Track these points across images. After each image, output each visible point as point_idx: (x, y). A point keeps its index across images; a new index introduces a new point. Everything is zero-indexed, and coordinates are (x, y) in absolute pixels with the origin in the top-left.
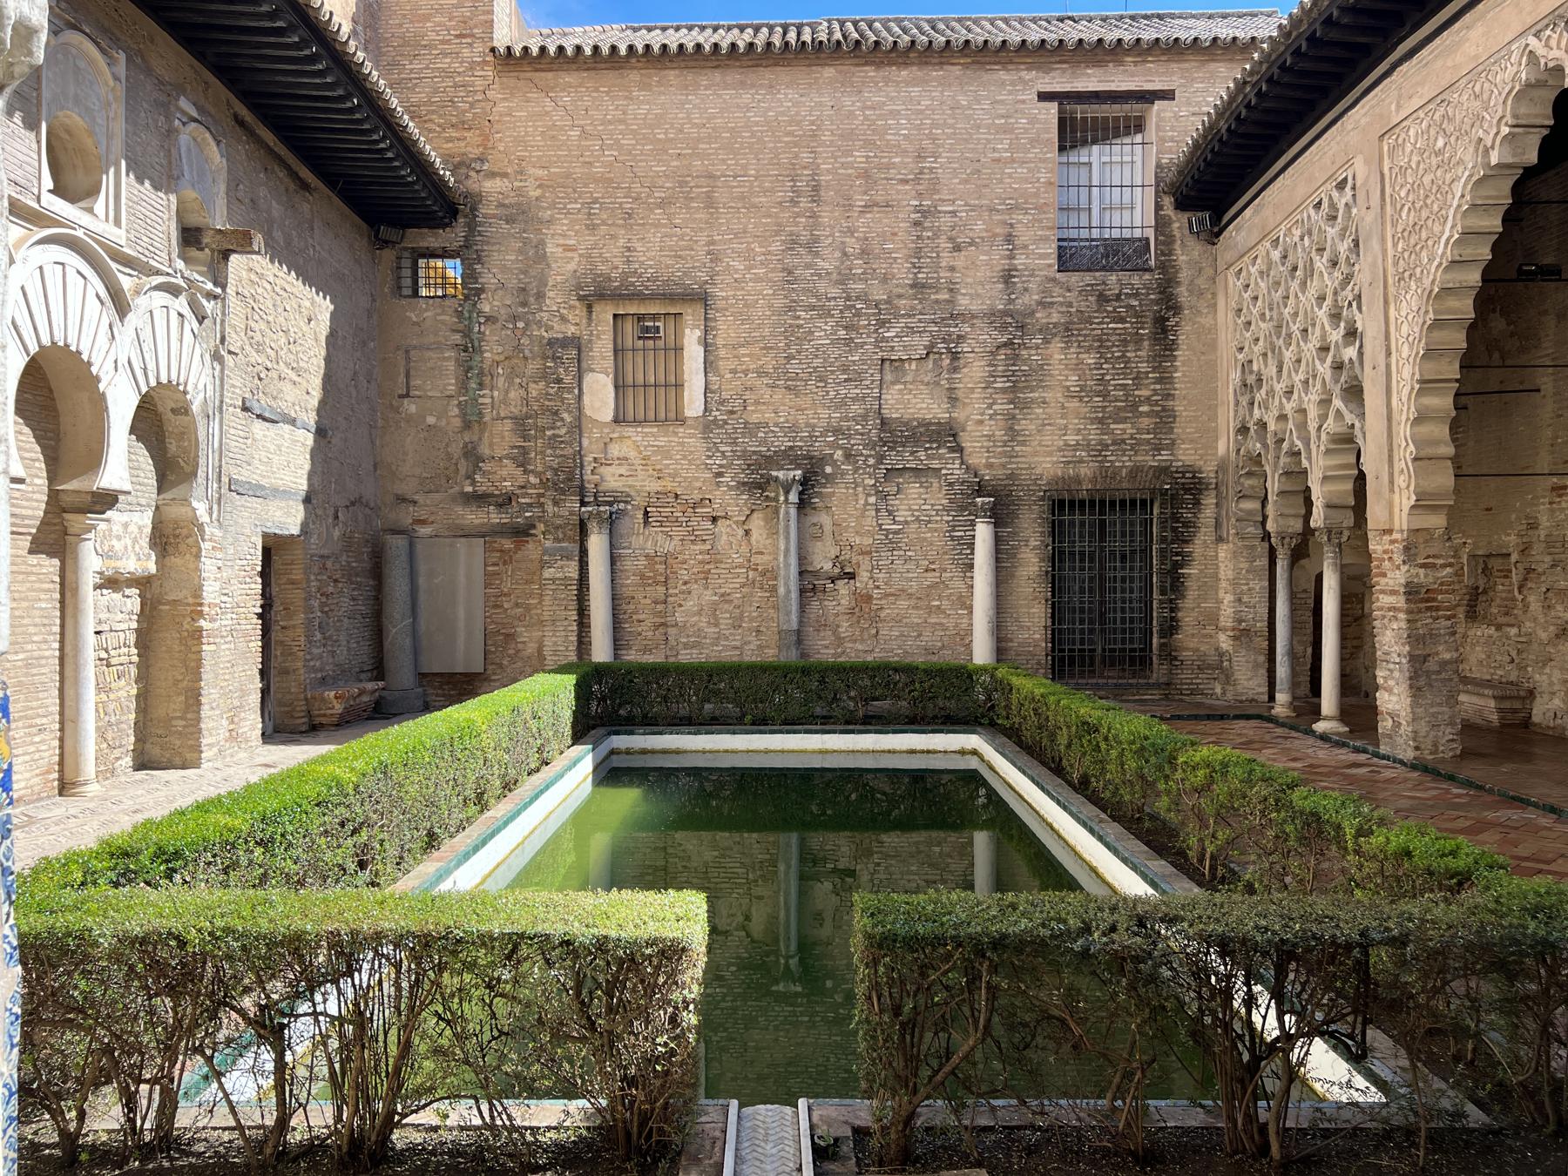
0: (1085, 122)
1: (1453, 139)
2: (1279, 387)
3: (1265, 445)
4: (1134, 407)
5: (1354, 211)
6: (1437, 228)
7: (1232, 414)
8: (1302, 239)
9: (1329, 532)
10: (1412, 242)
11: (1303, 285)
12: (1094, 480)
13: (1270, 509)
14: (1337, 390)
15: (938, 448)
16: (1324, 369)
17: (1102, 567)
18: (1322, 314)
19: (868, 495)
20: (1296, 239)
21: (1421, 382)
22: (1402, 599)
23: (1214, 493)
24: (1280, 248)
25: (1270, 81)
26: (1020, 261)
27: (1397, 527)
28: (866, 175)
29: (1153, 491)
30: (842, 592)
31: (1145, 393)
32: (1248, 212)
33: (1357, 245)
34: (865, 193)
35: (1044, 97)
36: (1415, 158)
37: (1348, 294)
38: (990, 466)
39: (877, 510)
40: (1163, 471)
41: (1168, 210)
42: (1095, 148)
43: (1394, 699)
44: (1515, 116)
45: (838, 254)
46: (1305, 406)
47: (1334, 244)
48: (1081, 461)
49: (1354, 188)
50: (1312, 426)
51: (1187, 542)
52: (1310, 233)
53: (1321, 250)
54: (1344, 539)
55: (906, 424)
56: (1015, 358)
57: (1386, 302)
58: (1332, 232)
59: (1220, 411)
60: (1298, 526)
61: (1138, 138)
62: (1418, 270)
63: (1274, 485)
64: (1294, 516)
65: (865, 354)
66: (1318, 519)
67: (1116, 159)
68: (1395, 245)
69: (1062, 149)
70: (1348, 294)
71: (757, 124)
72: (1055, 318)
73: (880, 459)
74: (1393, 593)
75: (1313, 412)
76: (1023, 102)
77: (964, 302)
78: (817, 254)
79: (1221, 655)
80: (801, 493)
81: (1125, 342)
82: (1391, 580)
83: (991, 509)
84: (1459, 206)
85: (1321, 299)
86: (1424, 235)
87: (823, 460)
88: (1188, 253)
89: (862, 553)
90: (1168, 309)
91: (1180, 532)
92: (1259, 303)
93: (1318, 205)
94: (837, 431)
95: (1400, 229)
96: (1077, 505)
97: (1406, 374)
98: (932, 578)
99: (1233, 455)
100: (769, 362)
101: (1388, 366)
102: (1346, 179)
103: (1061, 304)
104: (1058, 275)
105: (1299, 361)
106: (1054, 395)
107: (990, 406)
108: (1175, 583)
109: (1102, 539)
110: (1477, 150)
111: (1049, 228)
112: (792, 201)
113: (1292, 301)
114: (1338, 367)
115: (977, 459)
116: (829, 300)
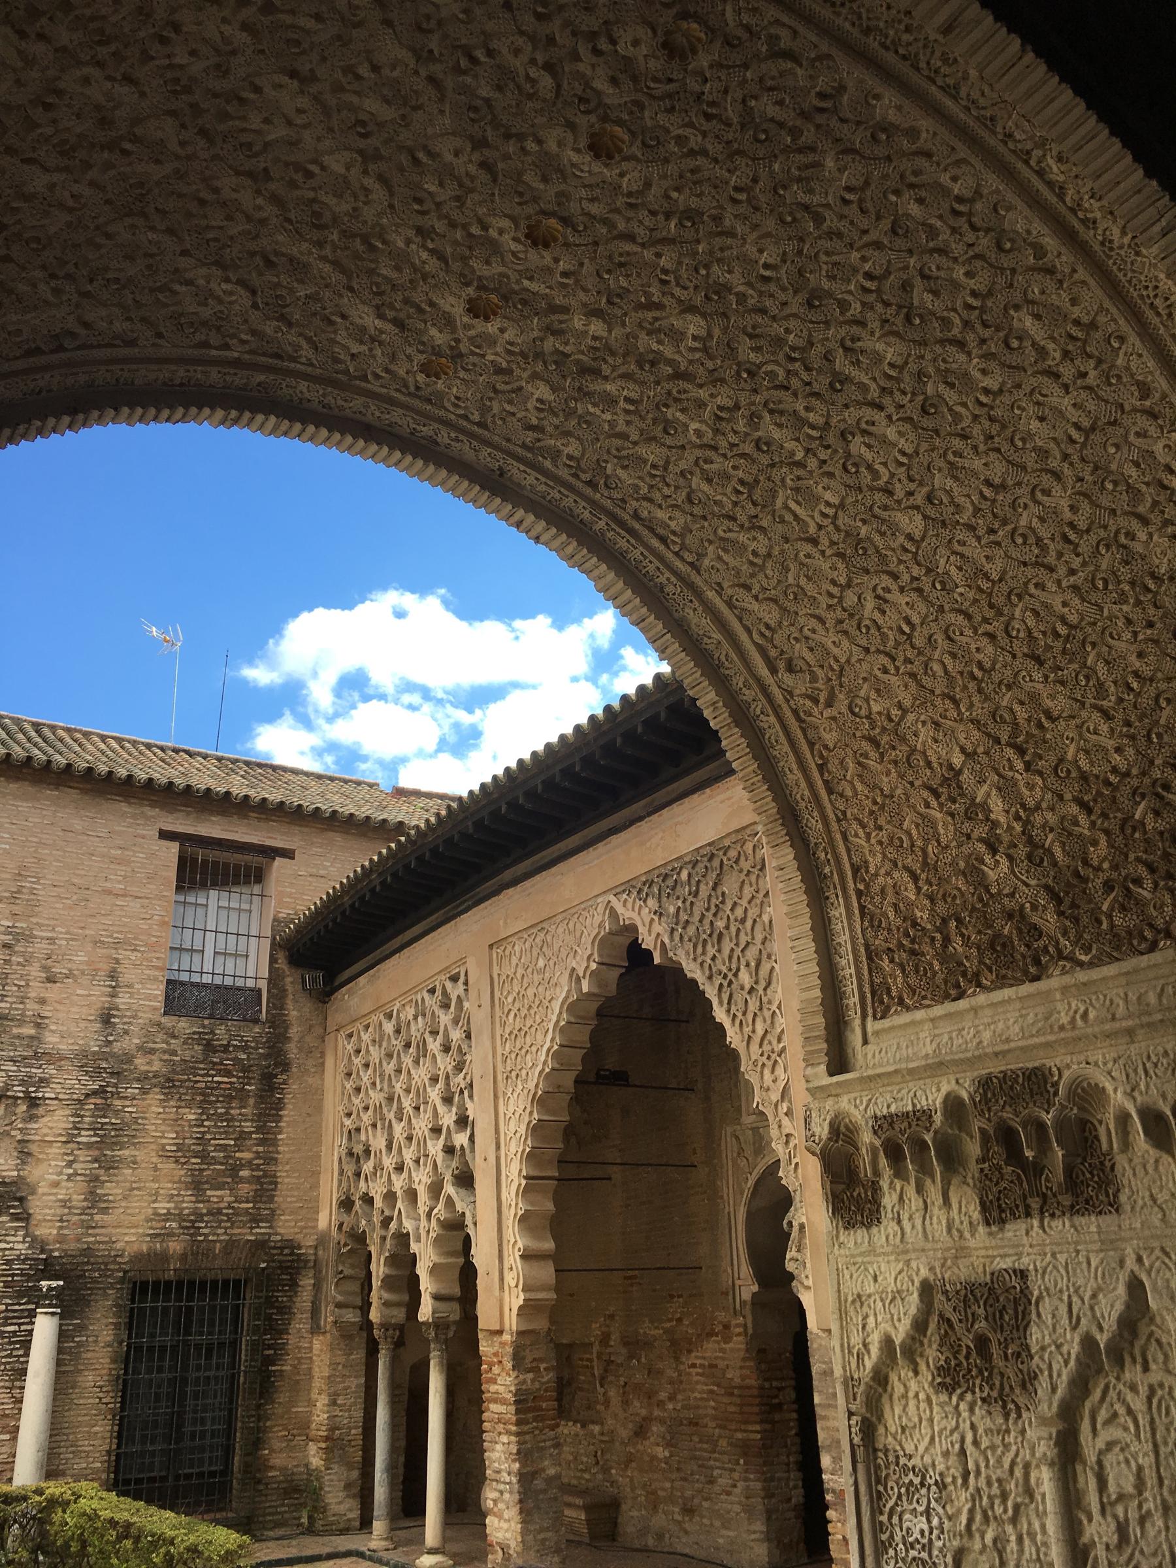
0: (207, 868)
2: (388, 1162)
3: (369, 1221)
4: (234, 1170)
5: (466, 1005)
6: (540, 1036)
8: (416, 1018)
10: (518, 1046)
12: (183, 1257)
13: (376, 1295)
14: (448, 1177)
16: (435, 1148)
17: (185, 1368)
20: (411, 1017)
22: (512, 1409)
23: (311, 1273)
24: (394, 1021)
25: (395, 875)
26: (122, 1000)
27: (507, 1327)
31: (247, 1155)
32: (362, 980)
33: (468, 1036)
35: (165, 835)
36: (520, 971)
37: (459, 1080)
40: (261, 1245)
41: (282, 964)
42: (213, 893)
43: (505, 1525)
44: (600, 955)
49: (466, 983)
50: (422, 1208)
52: (424, 1015)
53: (435, 1033)
54: (451, 1334)
58: (445, 1018)
61: (257, 889)
62: (524, 1072)
63: (379, 1269)
64: (398, 1304)
66: (426, 1310)
69: (179, 888)
70: (459, 1080)
72: (157, 1066)
74: (503, 1402)
75: (423, 1197)
76: (143, 837)
77: (51, 1040)
82: (501, 1385)
83: (57, 1297)
84: (558, 1022)
85: (434, 1080)
88: (297, 1011)
90: (276, 1065)
91: (274, 1322)
95: (507, 1031)
96: (162, 1288)
97: (515, 1172)
101: (498, 1159)
103: (165, 1052)
104: (163, 1020)
108: (265, 1383)
109: (187, 1332)
110: (571, 976)
113: (404, 1075)
114: (449, 1150)
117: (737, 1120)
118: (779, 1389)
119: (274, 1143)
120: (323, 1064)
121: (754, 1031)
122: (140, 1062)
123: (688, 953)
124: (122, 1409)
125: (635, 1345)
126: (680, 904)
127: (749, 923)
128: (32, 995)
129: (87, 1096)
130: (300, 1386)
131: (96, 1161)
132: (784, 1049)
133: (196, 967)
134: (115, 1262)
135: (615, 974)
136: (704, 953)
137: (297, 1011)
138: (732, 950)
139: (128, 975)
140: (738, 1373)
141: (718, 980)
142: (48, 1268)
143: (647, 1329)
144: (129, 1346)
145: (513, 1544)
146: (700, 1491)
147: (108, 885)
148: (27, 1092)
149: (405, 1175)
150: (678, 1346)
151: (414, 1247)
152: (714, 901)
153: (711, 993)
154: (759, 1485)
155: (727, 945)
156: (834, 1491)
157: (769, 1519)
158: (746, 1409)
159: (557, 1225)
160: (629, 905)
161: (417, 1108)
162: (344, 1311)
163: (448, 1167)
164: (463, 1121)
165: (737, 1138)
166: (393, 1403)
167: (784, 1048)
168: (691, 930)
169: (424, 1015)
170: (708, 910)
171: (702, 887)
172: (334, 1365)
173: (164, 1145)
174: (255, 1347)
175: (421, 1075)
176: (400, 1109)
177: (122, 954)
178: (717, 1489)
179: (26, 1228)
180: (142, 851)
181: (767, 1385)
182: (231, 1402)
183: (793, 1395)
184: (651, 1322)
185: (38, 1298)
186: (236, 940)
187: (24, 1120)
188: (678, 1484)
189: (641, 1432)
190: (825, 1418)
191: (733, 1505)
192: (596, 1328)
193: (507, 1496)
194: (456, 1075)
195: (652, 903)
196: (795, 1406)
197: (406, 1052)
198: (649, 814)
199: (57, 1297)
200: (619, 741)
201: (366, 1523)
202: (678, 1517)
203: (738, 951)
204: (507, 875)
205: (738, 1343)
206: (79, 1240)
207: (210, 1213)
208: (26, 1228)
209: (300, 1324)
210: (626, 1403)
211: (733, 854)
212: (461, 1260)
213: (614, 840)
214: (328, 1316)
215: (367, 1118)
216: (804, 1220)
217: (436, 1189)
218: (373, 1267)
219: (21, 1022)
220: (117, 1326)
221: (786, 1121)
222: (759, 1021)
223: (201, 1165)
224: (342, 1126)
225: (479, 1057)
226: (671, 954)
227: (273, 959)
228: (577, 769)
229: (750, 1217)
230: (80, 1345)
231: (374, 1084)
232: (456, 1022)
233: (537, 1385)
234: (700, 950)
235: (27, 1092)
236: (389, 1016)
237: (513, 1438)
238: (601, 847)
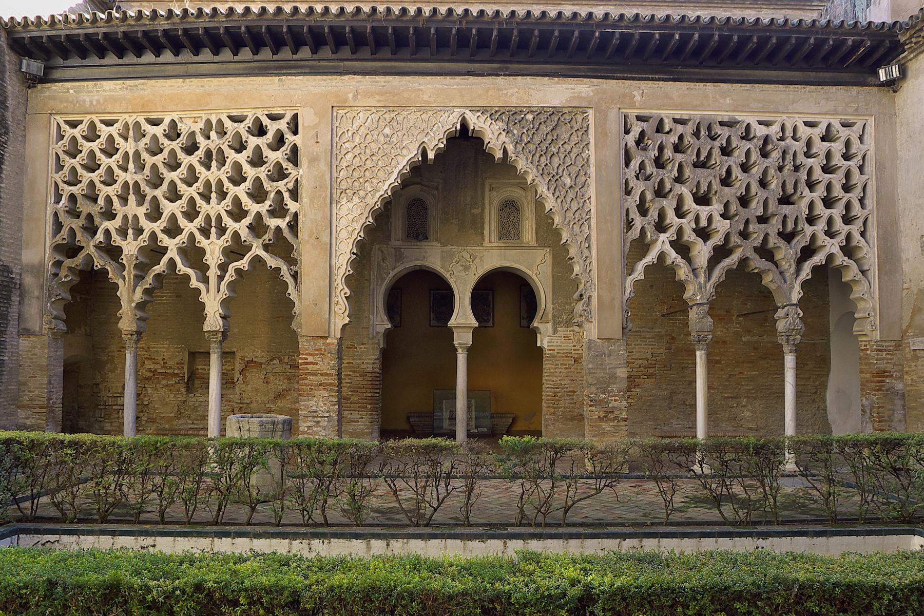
6: (381, 175)
27: (332, 334)
127: (573, 155)
152: (550, 137)
155: (556, 161)
168: (532, 147)
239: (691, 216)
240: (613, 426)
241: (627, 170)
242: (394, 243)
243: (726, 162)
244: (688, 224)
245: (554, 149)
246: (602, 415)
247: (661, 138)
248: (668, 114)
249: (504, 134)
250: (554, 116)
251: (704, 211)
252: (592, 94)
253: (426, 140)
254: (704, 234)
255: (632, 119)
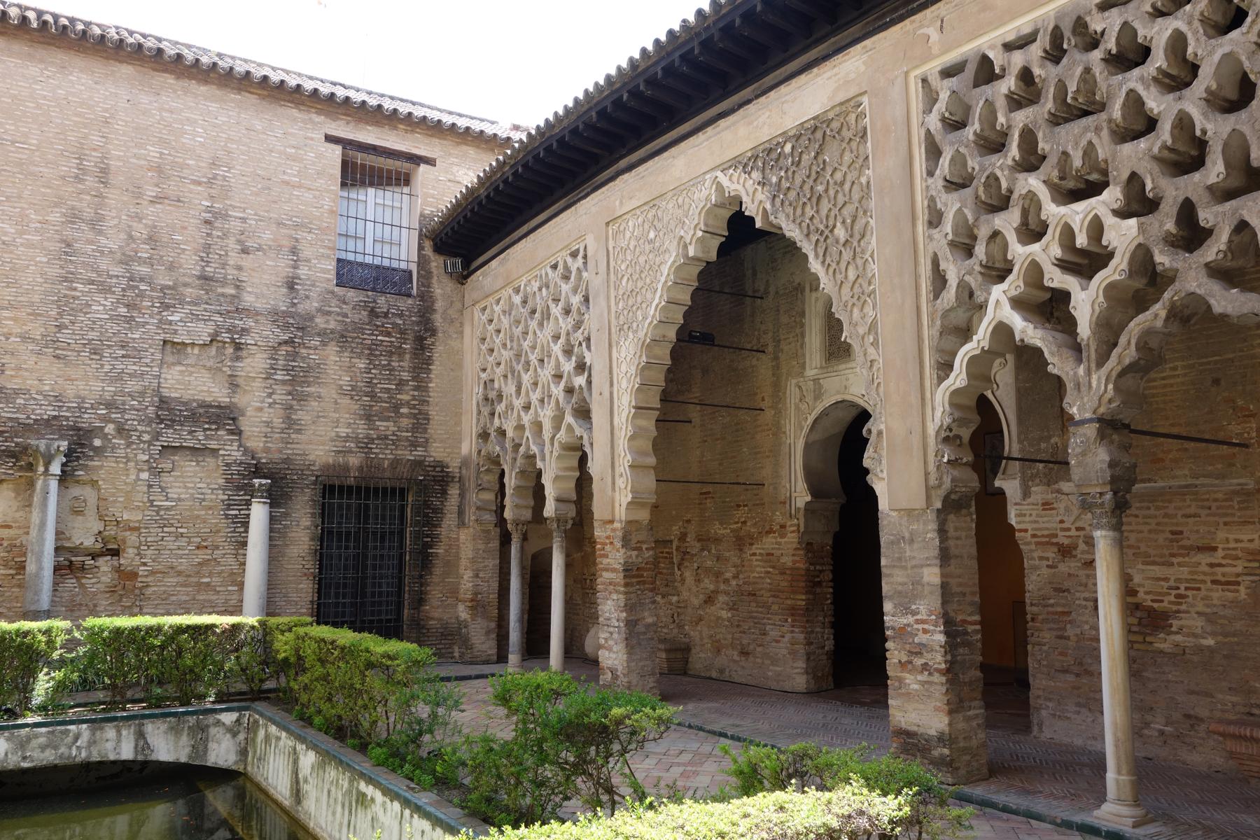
0: (364, 170)
1: (661, 234)
2: (518, 403)
3: (503, 448)
4: (396, 408)
5: (585, 274)
6: (649, 296)
7: (474, 421)
8: (540, 289)
9: (558, 520)
10: (630, 303)
11: (541, 325)
12: (360, 468)
13: (507, 501)
15: (217, 429)
16: (558, 391)
17: (365, 547)
18: (557, 349)
19: (141, 470)
20: (535, 289)
21: (637, 408)
22: (622, 575)
23: (457, 485)
24: (521, 294)
25: (525, 166)
27: (617, 517)
28: (159, 169)
29: (409, 480)
30: (104, 568)
31: (405, 397)
32: (494, 263)
34: (157, 185)
35: (330, 139)
37: (579, 336)
38: (267, 450)
39: (150, 486)
40: (418, 464)
41: (428, 251)
42: (371, 191)
43: (614, 656)
44: (706, 225)
45: (123, 236)
46: (541, 419)
47: (567, 296)
48: (351, 452)
49: (585, 257)
50: (547, 435)
51: (436, 526)
52: (548, 287)
53: (556, 301)
54: (569, 526)
55: (185, 404)
56: (294, 356)
57: (610, 345)
58: (565, 288)
59: (464, 419)
60: (527, 515)
61: (406, 190)
63: (510, 482)
64: (526, 507)
65: (146, 333)
66: (549, 510)
67: (389, 203)
68: (617, 304)
69: (344, 185)
70: (579, 336)
71: (44, 97)
72: (332, 325)
73: (156, 436)
74: (614, 570)
76: (312, 139)
77: (249, 300)
78: (100, 232)
79: (459, 623)
80: (63, 465)
81: (391, 353)
82: (612, 560)
83: (267, 491)
85: (556, 337)
86: (639, 299)
87: (91, 432)
88: (442, 288)
89: (131, 529)
90: (426, 330)
91: (430, 517)
92: (501, 335)
93: (555, 267)
94: (110, 405)
95: (621, 292)
98: (203, 555)
99: (475, 455)
100: (37, 330)
101: (611, 393)
102: (578, 250)
103: (338, 314)
104: (337, 289)
105: (536, 384)
106: (329, 392)
107: (270, 395)
108: (425, 560)
109: (366, 522)
111: (329, 248)
112: (76, 177)
113: (530, 336)
114: (570, 391)
115: (255, 444)
116: (111, 277)
117: (801, 374)
118: (821, 571)
119: (426, 389)
120: (462, 333)
121: (846, 277)
122: (320, 321)
123: (788, 216)
124: (320, 573)
125: (706, 540)
126: (782, 174)
128: (231, 263)
129: (280, 344)
130: (451, 566)
131: (290, 394)
132: (874, 291)
133: (360, 249)
134: (308, 469)
135: (716, 243)
136: (803, 213)
137: (442, 288)
138: (830, 210)
139: (306, 252)
140: (791, 558)
141: (814, 238)
142: (258, 471)
143: (718, 529)
144: (322, 529)
145: (620, 668)
146: (754, 640)
147: (286, 177)
148: (233, 339)
149: (532, 411)
150: (741, 542)
151: (539, 464)
152: (814, 168)
153: (807, 248)
154: (802, 636)
155: (825, 206)
156: (893, 628)
157: (808, 659)
158: (795, 584)
159: (659, 446)
160: (735, 179)
161: (542, 361)
162: (482, 513)
163: (568, 402)
164: (581, 367)
165: (800, 387)
166: (522, 576)
167: (874, 291)
169: (548, 287)
170: (808, 177)
171: (805, 157)
172: (476, 550)
173: (341, 386)
174: (417, 536)
175: (545, 335)
176: (528, 363)
177: (300, 235)
178: (768, 638)
179: (239, 440)
180: (311, 150)
181: (812, 568)
182: (400, 572)
183: (831, 576)
184: (721, 524)
185: (251, 492)
186: (390, 228)
187: (232, 360)
188: (737, 635)
189: (709, 600)
190: (889, 575)
191: (782, 650)
192: (676, 530)
193: (615, 636)
194: (575, 331)
195: (756, 175)
196: (831, 584)
197: (532, 319)
198: (757, 97)
199: (267, 491)
200: (738, 21)
201: (502, 658)
202: (736, 658)
203: (835, 211)
204: (623, 163)
205: (791, 539)
206: (280, 452)
207: (378, 438)
208: (239, 440)
209: (449, 520)
210: (698, 581)
211: (835, 125)
212: (578, 474)
213: (723, 123)
214: (471, 516)
215: (499, 371)
216: (882, 427)
217: (558, 420)
218: (506, 480)
219: (224, 283)
220: (313, 515)
221: (871, 350)
222: (851, 268)
223: (371, 402)
224: (479, 378)
225: (594, 320)
226: (772, 218)
227: (421, 248)
228: (696, 52)
229: (807, 446)
230: (285, 527)
231: (504, 345)
232: (575, 291)
233: (640, 560)
234: (799, 211)
235: (233, 339)
236: (517, 291)
237: (621, 596)
238: (710, 131)
239: (1052, 236)
240: (923, 683)
241: (930, 181)
242: (810, 373)
243: (1120, 85)
244: (1047, 251)
245: (820, 188)
246: (904, 659)
247: (987, 90)
248: (989, 42)
249: (760, 188)
250: (817, 132)
251: (1078, 214)
252: (863, 68)
253: (682, 233)
254: (1086, 262)
255: (935, 81)
